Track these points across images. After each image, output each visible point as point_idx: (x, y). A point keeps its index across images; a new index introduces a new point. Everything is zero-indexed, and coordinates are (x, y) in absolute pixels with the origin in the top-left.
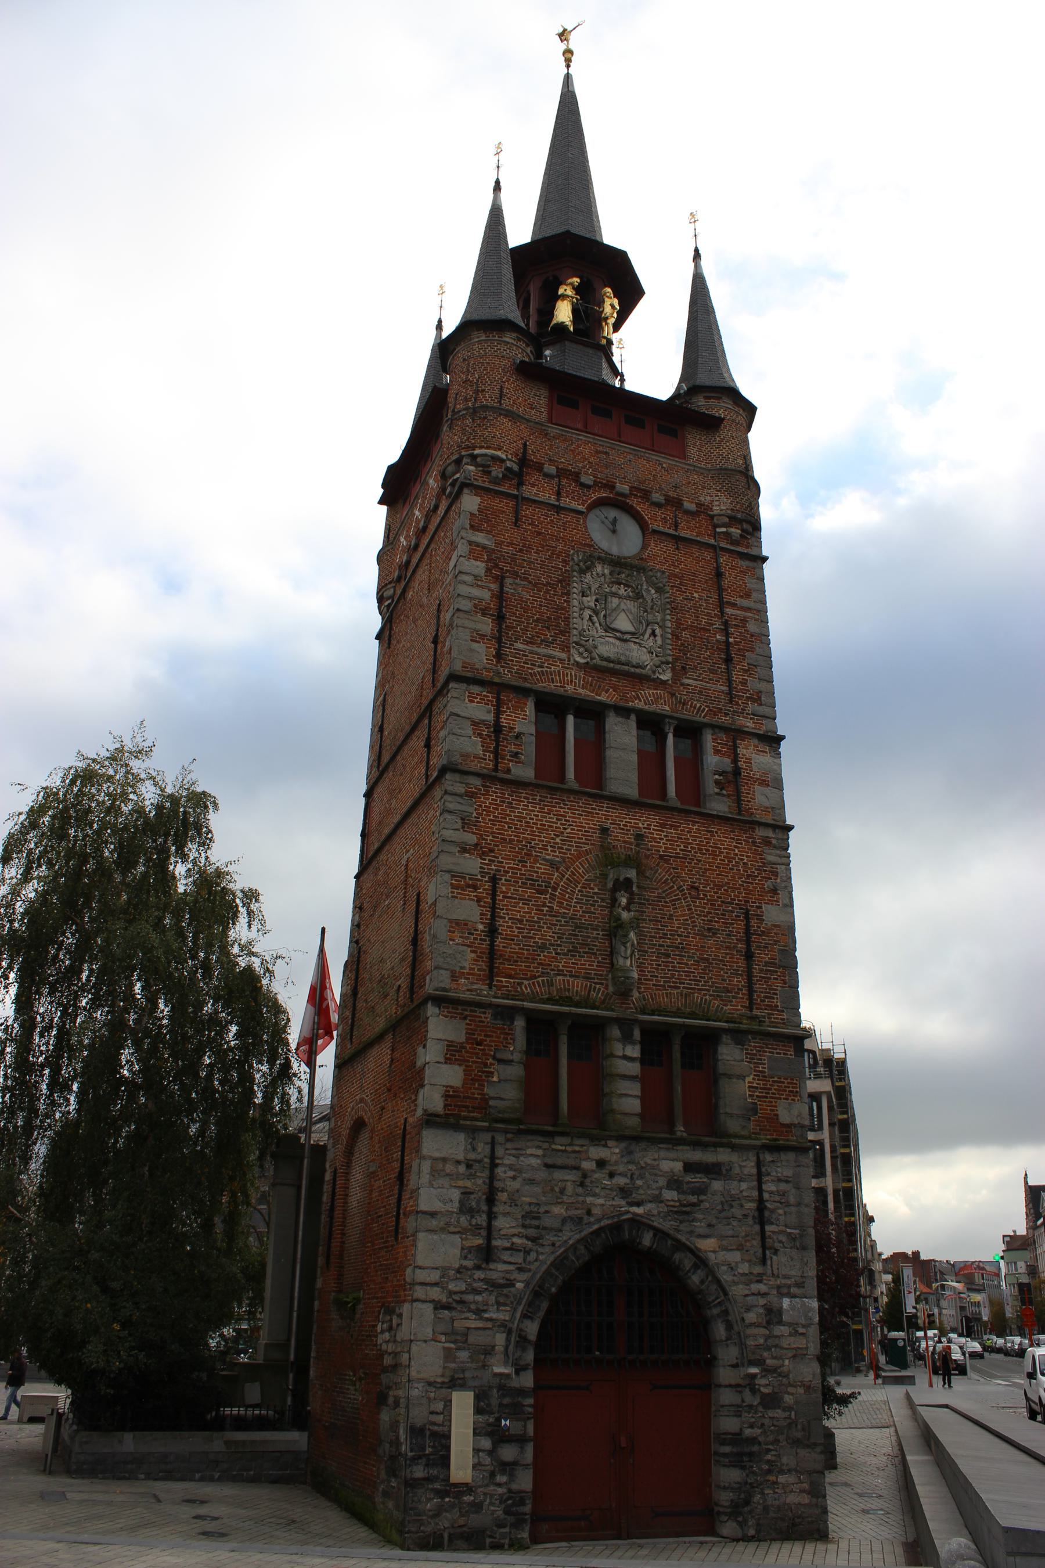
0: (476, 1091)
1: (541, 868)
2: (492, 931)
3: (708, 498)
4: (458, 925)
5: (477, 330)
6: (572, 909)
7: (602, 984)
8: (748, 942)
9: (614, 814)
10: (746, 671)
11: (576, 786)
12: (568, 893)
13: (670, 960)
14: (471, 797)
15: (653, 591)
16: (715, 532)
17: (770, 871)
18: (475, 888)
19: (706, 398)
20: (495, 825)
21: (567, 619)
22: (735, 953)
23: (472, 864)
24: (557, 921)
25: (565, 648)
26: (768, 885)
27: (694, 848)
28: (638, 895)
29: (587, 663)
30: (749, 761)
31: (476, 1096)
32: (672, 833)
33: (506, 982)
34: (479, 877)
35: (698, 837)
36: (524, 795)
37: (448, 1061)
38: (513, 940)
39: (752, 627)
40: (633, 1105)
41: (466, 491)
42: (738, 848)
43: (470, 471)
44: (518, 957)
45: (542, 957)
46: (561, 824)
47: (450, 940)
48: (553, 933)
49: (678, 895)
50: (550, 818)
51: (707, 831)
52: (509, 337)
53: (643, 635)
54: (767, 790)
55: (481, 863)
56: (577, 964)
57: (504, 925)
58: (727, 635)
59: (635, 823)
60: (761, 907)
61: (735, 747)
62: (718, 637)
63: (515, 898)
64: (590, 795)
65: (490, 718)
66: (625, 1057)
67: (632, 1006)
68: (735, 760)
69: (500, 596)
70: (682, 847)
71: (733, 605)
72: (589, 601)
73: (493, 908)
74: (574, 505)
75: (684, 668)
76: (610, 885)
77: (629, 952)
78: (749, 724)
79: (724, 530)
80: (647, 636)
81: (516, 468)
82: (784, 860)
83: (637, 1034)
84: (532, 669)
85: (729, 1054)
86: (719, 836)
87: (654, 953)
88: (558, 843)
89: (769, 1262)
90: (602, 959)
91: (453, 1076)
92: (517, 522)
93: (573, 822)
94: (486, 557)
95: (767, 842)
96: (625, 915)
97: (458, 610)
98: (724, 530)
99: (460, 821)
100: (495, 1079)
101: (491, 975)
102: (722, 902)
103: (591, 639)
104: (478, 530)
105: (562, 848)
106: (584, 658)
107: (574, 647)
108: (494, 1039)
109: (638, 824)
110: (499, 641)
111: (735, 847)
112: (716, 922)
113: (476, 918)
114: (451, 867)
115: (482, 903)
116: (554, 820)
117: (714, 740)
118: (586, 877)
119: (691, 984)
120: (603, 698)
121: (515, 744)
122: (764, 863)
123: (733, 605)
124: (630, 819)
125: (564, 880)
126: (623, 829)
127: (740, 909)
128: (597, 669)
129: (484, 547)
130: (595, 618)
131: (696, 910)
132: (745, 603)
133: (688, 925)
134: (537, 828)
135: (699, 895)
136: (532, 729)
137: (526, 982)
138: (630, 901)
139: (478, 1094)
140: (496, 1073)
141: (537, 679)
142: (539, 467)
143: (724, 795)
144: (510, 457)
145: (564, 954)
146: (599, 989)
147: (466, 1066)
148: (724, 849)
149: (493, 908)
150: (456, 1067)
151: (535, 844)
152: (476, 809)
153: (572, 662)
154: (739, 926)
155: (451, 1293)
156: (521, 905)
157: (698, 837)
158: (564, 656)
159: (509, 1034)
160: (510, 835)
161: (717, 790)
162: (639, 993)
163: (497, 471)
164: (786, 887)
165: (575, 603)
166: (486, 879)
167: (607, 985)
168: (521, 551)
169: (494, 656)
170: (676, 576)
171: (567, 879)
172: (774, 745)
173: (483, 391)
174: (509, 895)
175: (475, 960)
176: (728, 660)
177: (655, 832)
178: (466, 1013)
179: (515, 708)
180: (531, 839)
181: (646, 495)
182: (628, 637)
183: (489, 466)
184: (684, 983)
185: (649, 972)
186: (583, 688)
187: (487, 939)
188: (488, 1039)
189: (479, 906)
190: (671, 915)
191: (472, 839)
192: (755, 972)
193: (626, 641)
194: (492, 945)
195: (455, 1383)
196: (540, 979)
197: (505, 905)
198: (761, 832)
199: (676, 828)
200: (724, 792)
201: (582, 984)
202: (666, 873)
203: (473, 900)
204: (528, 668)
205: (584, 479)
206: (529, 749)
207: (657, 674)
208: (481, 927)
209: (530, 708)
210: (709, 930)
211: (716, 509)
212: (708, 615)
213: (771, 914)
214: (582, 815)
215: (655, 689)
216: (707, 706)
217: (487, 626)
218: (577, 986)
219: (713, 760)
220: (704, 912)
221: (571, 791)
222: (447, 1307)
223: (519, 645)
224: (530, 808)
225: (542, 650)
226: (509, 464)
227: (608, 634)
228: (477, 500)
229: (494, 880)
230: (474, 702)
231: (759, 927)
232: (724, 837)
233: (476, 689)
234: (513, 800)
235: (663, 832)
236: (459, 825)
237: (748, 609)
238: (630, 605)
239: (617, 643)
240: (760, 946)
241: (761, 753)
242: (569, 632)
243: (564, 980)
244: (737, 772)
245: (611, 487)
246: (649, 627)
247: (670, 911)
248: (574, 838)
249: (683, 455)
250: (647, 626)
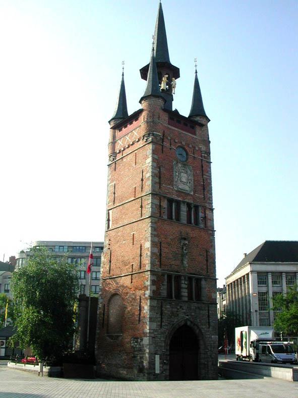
2: (160, 255)
8: (207, 258)
21: (173, 178)
26: (211, 244)
40: (186, 294)
57: (163, 255)
65: (159, 204)
66: (185, 284)
69: (160, 172)
72: (177, 174)
76: (182, 244)
96: (185, 252)
101: (161, 264)
120: (179, 199)
129: (156, 159)
155: (155, 335)
158: (172, 188)
195: (156, 354)
209: (166, 201)
213: (211, 251)
218: (176, 267)
219: (201, 215)
222: (154, 338)
223: (163, 185)
229: (161, 243)
237: (208, 176)
238: (185, 175)
244: (205, 217)
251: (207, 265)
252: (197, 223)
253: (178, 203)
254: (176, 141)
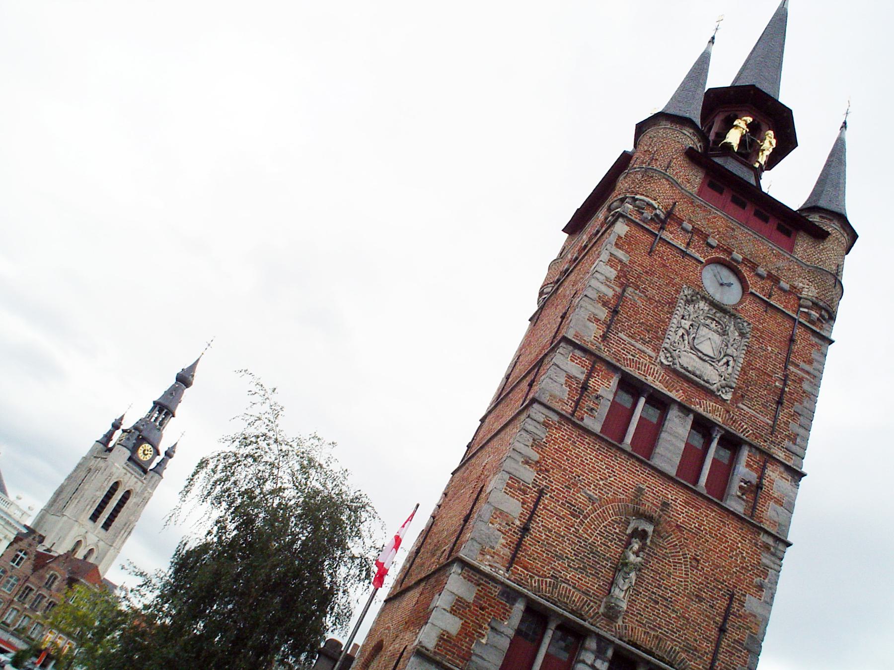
0: (466, 644)
1: (580, 498)
2: (525, 529)
3: (801, 285)
4: (500, 513)
5: (666, 120)
6: (593, 537)
7: (596, 603)
8: (725, 619)
9: (652, 480)
11: (629, 449)
12: (595, 524)
13: (657, 606)
14: (547, 427)
15: (737, 334)
16: (799, 310)
17: (762, 571)
18: (525, 493)
19: (820, 217)
20: (557, 454)
22: (712, 623)
23: (528, 475)
24: (578, 541)
25: (657, 349)
26: (757, 580)
27: (707, 530)
28: (650, 547)
29: (669, 365)
30: (772, 482)
31: (464, 648)
32: (692, 511)
33: (521, 571)
34: (530, 486)
35: (712, 523)
36: (587, 440)
37: (453, 611)
38: (539, 542)
39: (806, 386)
41: (620, 220)
42: (741, 542)
43: (628, 208)
44: (537, 556)
45: (556, 564)
46: (608, 472)
47: (491, 522)
48: (572, 549)
49: (681, 559)
50: (601, 464)
51: (720, 520)
52: (688, 131)
53: (719, 361)
54: (780, 509)
55: (536, 476)
56: (582, 580)
58: (785, 384)
59: (665, 493)
60: (745, 596)
61: (764, 468)
62: (777, 384)
63: (552, 512)
64: (638, 459)
65: (582, 377)
67: (614, 629)
68: (761, 477)
69: (620, 297)
70: (697, 525)
71: (797, 366)
72: (686, 324)
73: (533, 513)
74: (697, 255)
75: (742, 396)
76: (629, 531)
77: (625, 588)
78: (781, 455)
79: (806, 310)
80: (721, 363)
81: (662, 216)
82: (776, 567)
83: (610, 653)
84: (626, 355)
86: (730, 529)
87: (647, 596)
88: (600, 485)
90: (603, 584)
91: (453, 625)
92: (650, 253)
93: (617, 474)
94: (619, 268)
95: (767, 547)
96: (632, 558)
97: (586, 296)
98: (806, 310)
99: (531, 440)
100: (484, 641)
101: (512, 561)
102: (715, 579)
103: (678, 350)
104: (620, 248)
105: (602, 490)
106: (668, 361)
107: (663, 351)
108: (495, 610)
109: (668, 494)
110: (609, 327)
111: (739, 541)
112: (704, 592)
113: (517, 515)
114: (511, 471)
115: (526, 506)
116: (604, 467)
117: (749, 456)
118: (613, 518)
119: (667, 633)
120: (673, 395)
121: (594, 403)
122: (759, 563)
123: (797, 366)
124: (663, 488)
125: (595, 513)
126: (655, 494)
127: (728, 590)
128: (675, 371)
129: (621, 261)
130: (686, 337)
131: (691, 577)
132: (807, 367)
133: (681, 586)
134: (588, 468)
135: (698, 566)
136: (611, 397)
137: (537, 578)
138: (642, 549)
139: (466, 647)
140: (486, 637)
141: (627, 364)
142: (680, 222)
143: (743, 500)
144: (661, 207)
145: (574, 569)
146: (592, 607)
147: (465, 621)
148: (731, 540)
149: (533, 513)
150: (457, 619)
151: (582, 479)
152: (546, 437)
153: (658, 361)
154: (722, 604)
156: (555, 518)
157: (712, 523)
158: (653, 354)
159: (507, 611)
160: (566, 465)
161: (739, 494)
162: (623, 622)
163: (648, 214)
164: (770, 588)
165: (675, 321)
166: (535, 490)
167: (600, 606)
168: (647, 272)
169: (600, 336)
170: (758, 330)
171: (598, 514)
172: (796, 478)
173: (657, 159)
174: (549, 508)
175: (504, 545)
176: (779, 403)
177: (679, 506)
178: (481, 581)
179: (603, 377)
180: (581, 474)
181: (754, 267)
182: (707, 359)
183: (643, 209)
184: (662, 629)
185: (636, 609)
186: (660, 382)
187: (520, 533)
188: (490, 608)
189: (522, 507)
191: (536, 456)
193: (704, 361)
194: (521, 539)
196: (548, 580)
197: (542, 514)
198: (764, 538)
199: (697, 509)
200: (744, 497)
201: (580, 597)
202: (677, 539)
203: (520, 501)
204: (623, 353)
205: (711, 240)
206: (604, 410)
207: (720, 393)
208: (518, 523)
209: (614, 381)
210: (697, 596)
211: (804, 294)
213: (752, 603)
214: (626, 472)
215: (715, 403)
216: (751, 430)
217: (603, 313)
218: (576, 596)
219: (743, 471)
220: (697, 581)
221: (623, 451)
223: (621, 335)
224: (588, 451)
225: (639, 345)
226: (658, 212)
227: (692, 351)
228: (627, 228)
229: (541, 493)
230: (574, 362)
231: (739, 611)
232: (733, 530)
233: (578, 353)
234: (577, 440)
235: (686, 508)
236: (530, 444)
237: (808, 373)
238: (716, 338)
239: (697, 359)
240: (734, 626)
241: (784, 480)
242: (663, 340)
243: (567, 588)
244: (759, 486)
245: (729, 252)
246: (726, 358)
247: (670, 569)
248: (615, 486)
249: (791, 250)
250: (725, 356)
251: (718, 645)
253: (660, 402)
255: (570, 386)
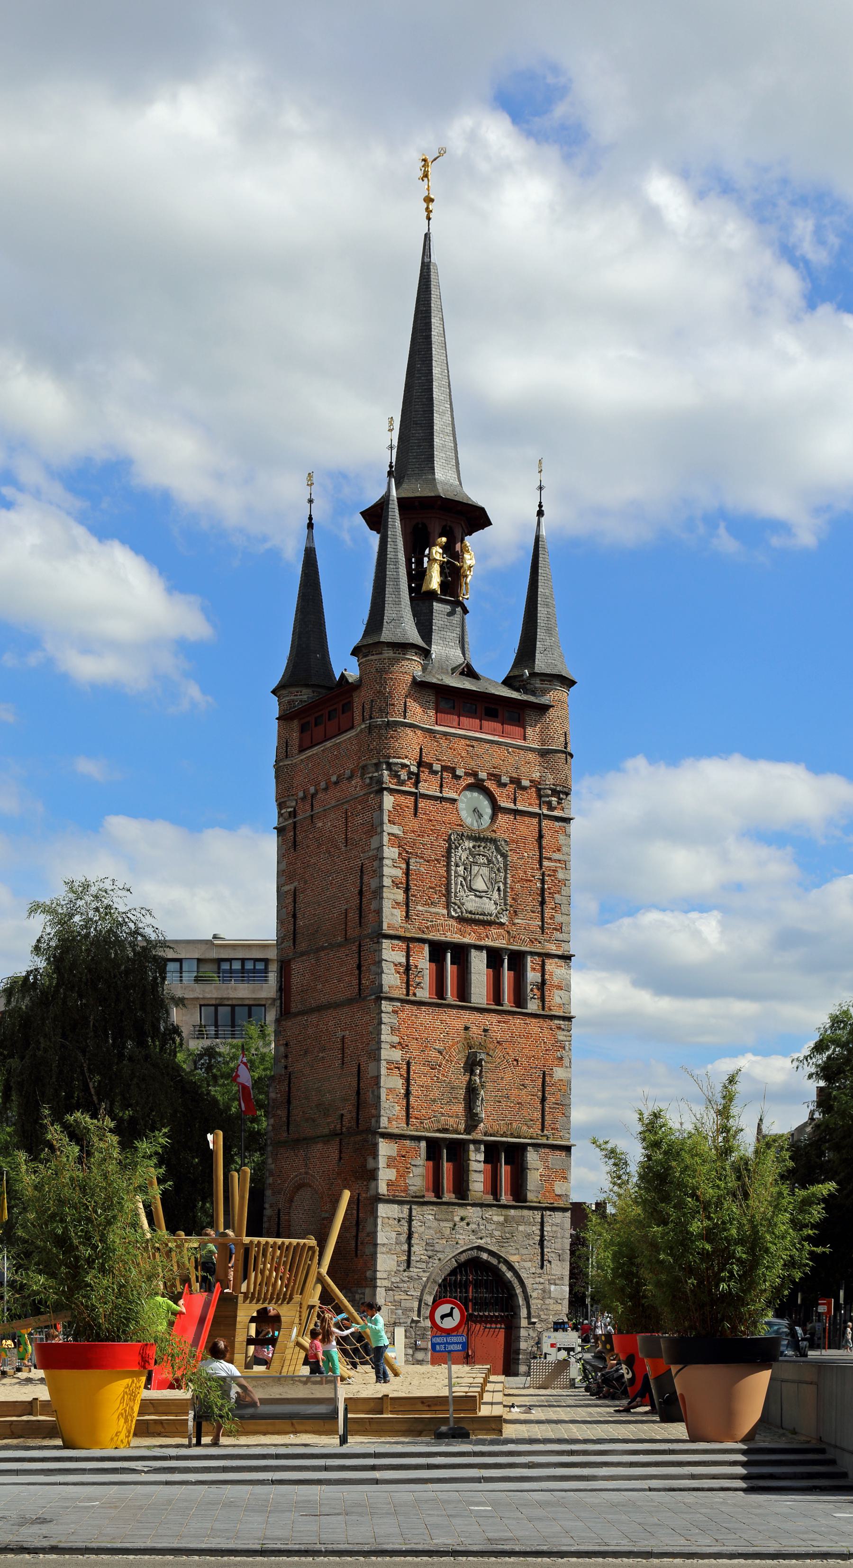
10: (553, 909)
54: (561, 993)
65: (403, 960)
69: (407, 873)
78: (552, 948)
85: (532, 1157)
89: (545, 1267)
104: (394, 824)
117: (532, 962)
120: (467, 940)
142: (430, 766)
176: (542, 903)
190: (502, 1078)
192: (547, 1109)
193: (481, 897)
210: (523, 1085)
212: (533, 869)
213: (559, 1073)
219: (532, 976)
223: (419, 908)
225: (433, 910)
233: (396, 942)
238: (485, 871)
239: (477, 899)
252: (520, 999)
254: (460, 772)
255: (399, 973)
